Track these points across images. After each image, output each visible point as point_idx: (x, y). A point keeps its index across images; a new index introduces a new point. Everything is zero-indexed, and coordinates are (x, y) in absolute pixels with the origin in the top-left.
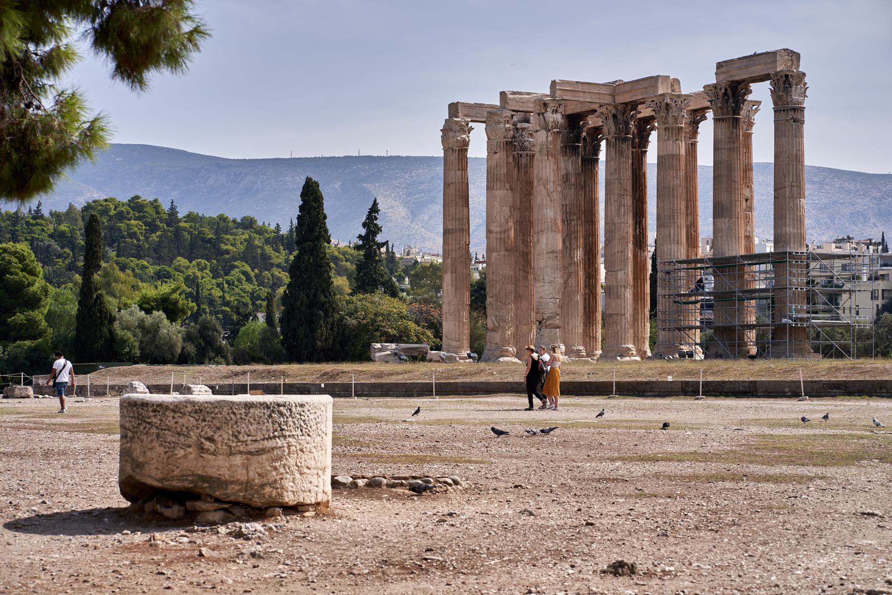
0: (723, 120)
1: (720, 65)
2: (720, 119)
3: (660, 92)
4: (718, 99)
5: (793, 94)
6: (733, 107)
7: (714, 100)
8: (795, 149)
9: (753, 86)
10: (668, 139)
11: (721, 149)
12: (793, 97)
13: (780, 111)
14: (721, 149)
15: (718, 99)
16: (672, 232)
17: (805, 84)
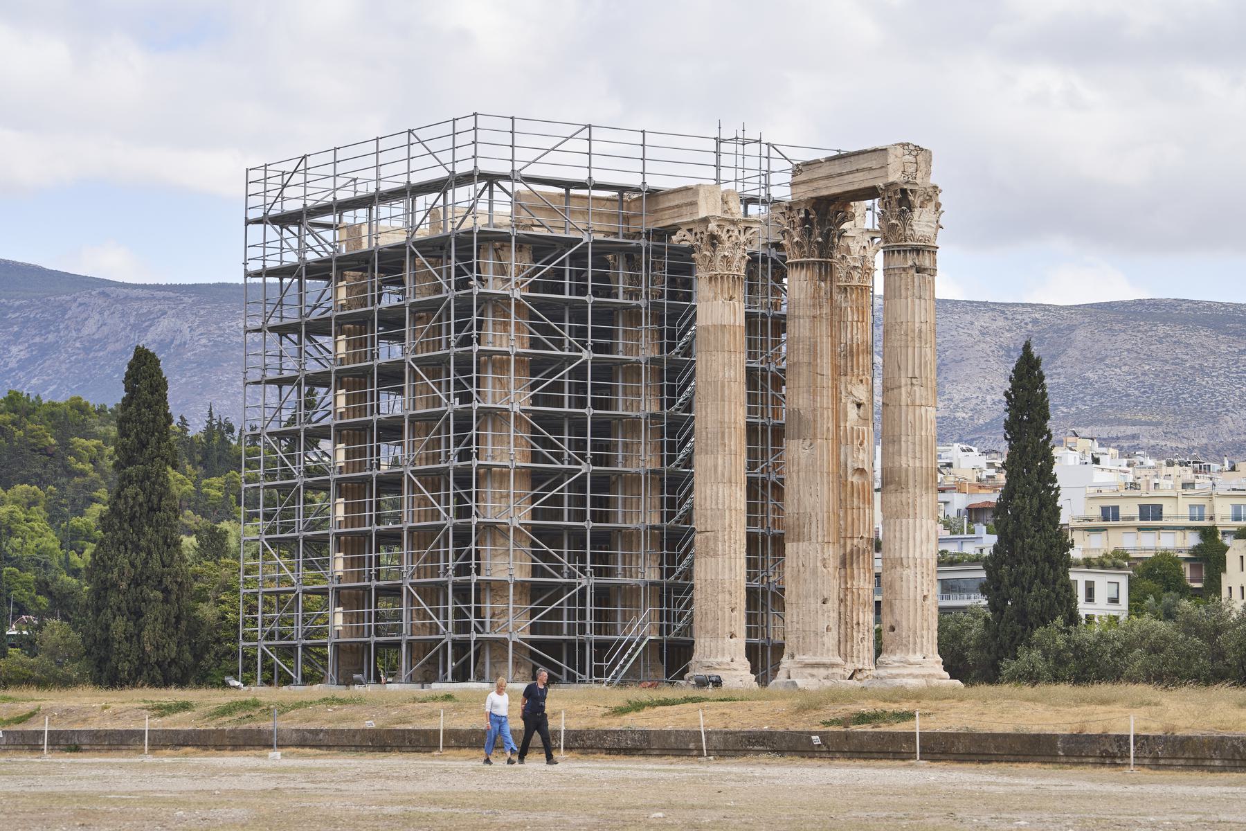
0: (802, 264)
1: (798, 169)
2: (797, 264)
3: (702, 214)
4: (794, 229)
5: (913, 223)
6: (818, 243)
7: (787, 231)
8: (917, 320)
9: (859, 207)
10: (715, 298)
11: (799, 318)
12: (914, 228)
13: (893, 252)
14: (799, 318)
15: (794, 229)
16: (720, 462)
17: (938, 206)
